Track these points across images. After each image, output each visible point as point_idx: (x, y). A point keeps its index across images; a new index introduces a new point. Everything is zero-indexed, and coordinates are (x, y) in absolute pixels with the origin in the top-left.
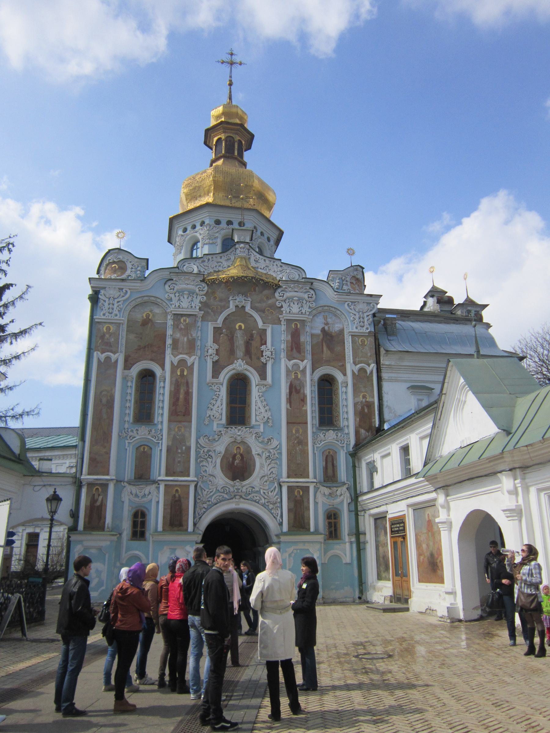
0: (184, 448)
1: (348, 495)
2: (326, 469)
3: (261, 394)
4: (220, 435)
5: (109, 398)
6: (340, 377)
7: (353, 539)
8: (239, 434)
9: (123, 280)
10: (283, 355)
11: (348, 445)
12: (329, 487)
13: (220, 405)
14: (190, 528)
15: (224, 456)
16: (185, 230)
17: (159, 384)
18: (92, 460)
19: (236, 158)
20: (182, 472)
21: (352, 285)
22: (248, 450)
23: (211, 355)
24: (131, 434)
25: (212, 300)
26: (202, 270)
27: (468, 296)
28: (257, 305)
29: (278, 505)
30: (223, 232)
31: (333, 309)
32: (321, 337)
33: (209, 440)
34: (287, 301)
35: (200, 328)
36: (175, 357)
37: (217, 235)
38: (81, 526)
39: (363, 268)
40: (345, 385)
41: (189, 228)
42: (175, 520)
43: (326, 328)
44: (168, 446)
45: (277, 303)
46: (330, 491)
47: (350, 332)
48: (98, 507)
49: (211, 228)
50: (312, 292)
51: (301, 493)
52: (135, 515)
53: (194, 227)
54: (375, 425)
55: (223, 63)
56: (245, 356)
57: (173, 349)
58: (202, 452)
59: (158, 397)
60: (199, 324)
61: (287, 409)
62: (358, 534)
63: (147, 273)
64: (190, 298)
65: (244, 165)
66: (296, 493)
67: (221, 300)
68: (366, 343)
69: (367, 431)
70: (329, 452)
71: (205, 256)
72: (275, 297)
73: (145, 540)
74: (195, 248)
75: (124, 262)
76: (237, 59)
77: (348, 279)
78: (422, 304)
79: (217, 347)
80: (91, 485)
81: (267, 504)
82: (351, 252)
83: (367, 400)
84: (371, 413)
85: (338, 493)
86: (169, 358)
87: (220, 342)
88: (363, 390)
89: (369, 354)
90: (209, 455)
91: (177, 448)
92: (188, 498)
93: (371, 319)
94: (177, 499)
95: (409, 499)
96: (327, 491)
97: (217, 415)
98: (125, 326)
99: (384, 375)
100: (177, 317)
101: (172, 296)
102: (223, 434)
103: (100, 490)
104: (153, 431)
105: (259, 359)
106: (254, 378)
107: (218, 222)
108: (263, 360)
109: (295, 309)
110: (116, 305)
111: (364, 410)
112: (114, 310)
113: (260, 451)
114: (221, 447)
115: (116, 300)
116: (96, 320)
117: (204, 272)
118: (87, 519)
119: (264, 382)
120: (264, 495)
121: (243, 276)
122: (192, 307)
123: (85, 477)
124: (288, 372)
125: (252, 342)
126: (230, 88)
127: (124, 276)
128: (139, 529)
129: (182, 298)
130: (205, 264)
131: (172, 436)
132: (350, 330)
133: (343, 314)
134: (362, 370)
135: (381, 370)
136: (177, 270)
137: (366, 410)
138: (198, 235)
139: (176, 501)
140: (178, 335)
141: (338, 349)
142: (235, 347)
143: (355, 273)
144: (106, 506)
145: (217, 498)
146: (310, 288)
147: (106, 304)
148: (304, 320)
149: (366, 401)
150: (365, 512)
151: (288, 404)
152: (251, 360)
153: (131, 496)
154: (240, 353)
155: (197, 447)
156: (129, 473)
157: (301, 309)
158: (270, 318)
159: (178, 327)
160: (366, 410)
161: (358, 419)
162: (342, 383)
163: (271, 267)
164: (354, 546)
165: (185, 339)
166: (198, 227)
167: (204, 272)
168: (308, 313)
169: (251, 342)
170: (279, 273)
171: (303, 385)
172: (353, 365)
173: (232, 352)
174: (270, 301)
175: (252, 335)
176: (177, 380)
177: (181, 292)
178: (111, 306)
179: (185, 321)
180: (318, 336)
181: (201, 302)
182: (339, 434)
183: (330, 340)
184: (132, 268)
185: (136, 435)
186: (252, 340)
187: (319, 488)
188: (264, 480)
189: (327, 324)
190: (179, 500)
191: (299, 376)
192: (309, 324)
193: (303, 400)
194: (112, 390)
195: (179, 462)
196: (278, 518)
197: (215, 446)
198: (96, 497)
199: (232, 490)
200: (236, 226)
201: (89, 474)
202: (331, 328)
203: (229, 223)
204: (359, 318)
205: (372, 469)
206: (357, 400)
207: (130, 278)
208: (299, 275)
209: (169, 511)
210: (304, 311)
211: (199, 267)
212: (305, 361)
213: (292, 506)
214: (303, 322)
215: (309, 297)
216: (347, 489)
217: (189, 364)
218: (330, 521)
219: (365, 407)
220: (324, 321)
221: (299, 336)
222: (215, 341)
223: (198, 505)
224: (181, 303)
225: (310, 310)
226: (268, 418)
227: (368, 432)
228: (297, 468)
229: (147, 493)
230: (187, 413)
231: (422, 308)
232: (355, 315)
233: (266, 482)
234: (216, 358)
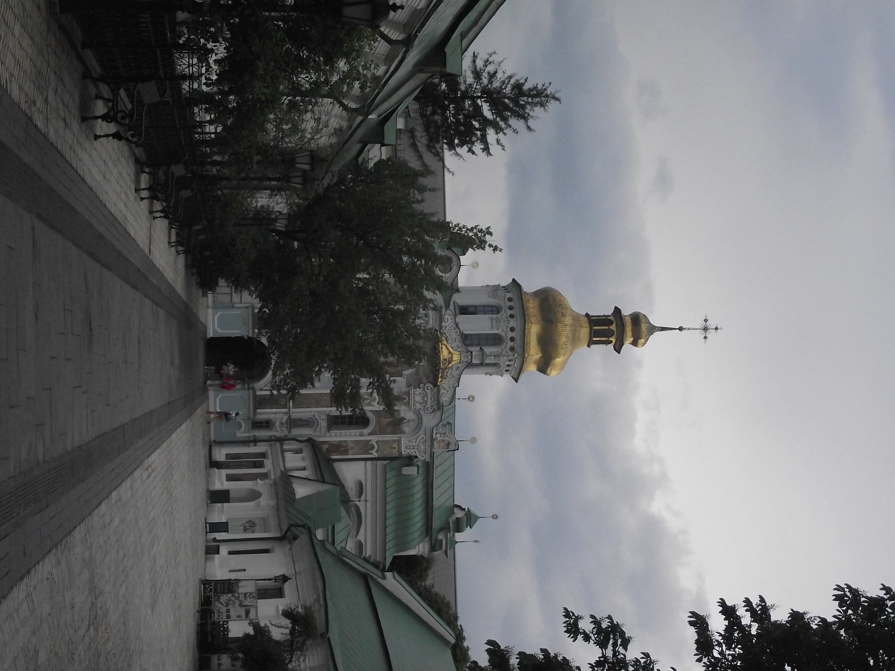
6: (366, 431)
7: (252, 439)
11: (317, 436)
16: (510, 300)
30: (503, 334)
53: (511, 308)
55: (706, 321)
62: (256, 441)
65: (588, 346)
69: (327, 450)
76: (711, 334)
77: (446, 438)
96: (284, 421)
99: (369, 463)
107: (512, 329)
134: (373, 447)
166: (510, 312)
174: (424, 379)
180: (399, 414)
200: (510, 344)
203: (512, 339)
214: (408, 404)
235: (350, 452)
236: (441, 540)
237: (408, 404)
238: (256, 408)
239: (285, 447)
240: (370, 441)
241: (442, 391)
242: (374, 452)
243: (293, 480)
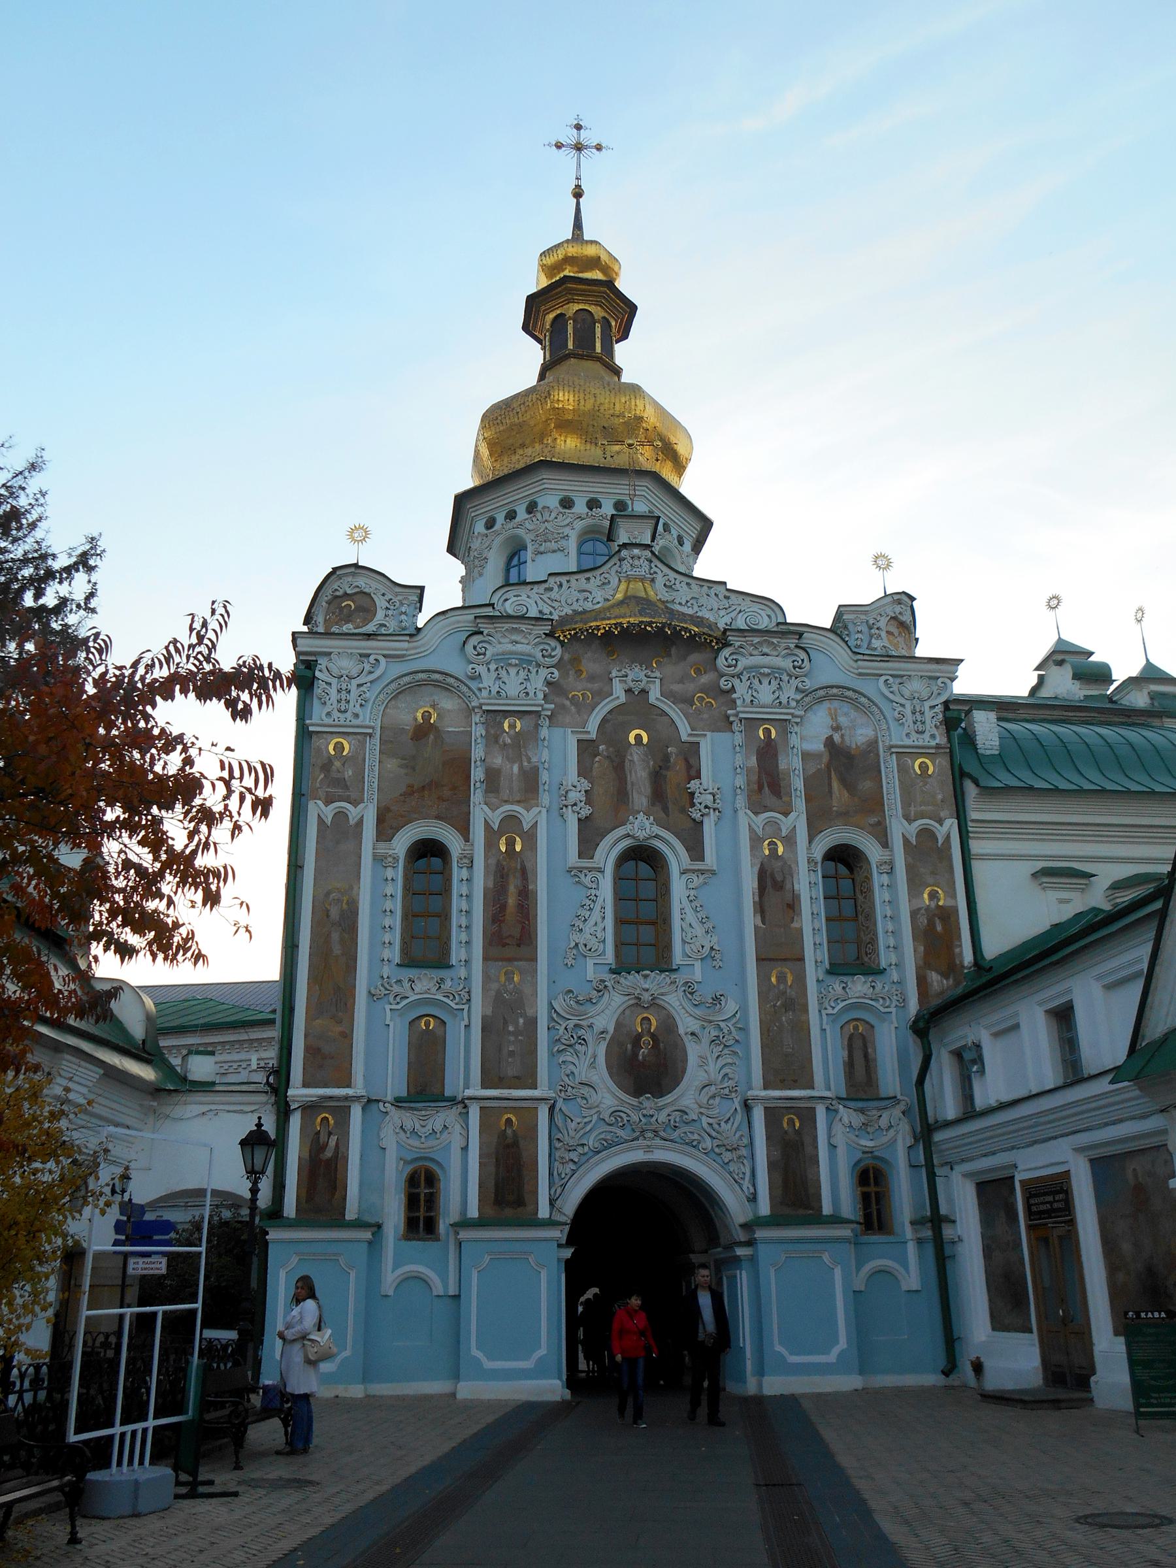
0: (521, 1021)
1: (907, 1128)
2: (850, 1065)
3: (692, 893)
4: (601, 988)
5: (345, 906)
6: (873, 851)
7: (928, 1233)
8: (647, 986)
9: (369, 636)
10: (741, 801)
12: (862, 1111)
13: (599, 920)
14: (544, 1212)
15: (612, 1038)
16: (490, 523)
17: (458, 873)
18: (312, 1051)
19: (598, 359)
20: (517, 1078)
21: (891, 638)
22: (669, 1025)
23: (575, 804)
24: (396, 989)
25: (571, 678)
26: (546, 610)
27: (1147, 660)
28: (676, 687)
29: (744, 1152)
30: (579, 525)
31: (850, 693)
32: (825, 759)
33: (577, 1002)
34: (744, 678)
35: (546, 743)
36: (493, 810)
37: (567, 531)
38: (290, 1207)
39: (913, 599)
40: (886, 868)
41: (500, 518)
42: (508, 1191)
43: (837, 738)
44: (483, 1018)
45: (722, 682)
46: (862, 1119)
47: (892, 747)
48: (329, 1161)
49: (553, 515)
50: (803, 655)
51: (797, 1125)
52: (412, 1180)
53: (511, 515)
54: (962, 962)
55: (559, 146)
56: (653, 804)
57: (486, 791)
58: (562, 1029)
59: (457, 904)
60: (544, 732)
61: (756, 927)
62: (935, 1220)
63: (421, 621)
64: (523, 674)
65: (617, 372)
66: (785, 1125)
67: (592, 678)
68: (930, 772)
69: (945, 975)
70: (856, 1028)
71: (552, 580)
72: (715, 668)
73: (438, 1240)
74: (515, 562)
75: (369, 594)
77: (882, 623)
78: (1034, 681)
79: (585, 785)
80: (310, 1109)
81: (717, 1150)
82: (882, 562)
83: (941, 903)
84: (952, 933)
85: (883, 1122)
86: (481, 814)
87: (594, 774)
88: (931, 880)
89: (940, 797)
90: (579, 1038)
91: (506, 1023)
92: (535, 1139)
93: (941, 716)
94: (509, 1141)
95: (1078, 1135)
97: (593, 943)
98: (377, 740)
99: (975, 846)
100: (494, 717)
101: (482, 669)
102: (611, 988)
103: (332, 1122)
104: (449, 983)
105: (683, 811)
106: (676, 856)
107: (567, 503)
108: (696, 815)
109: (766, 694)
110: (355, 692)
111: (934, 927)
112: (352, 704)
113: (694, 1025)
114: (605, 1016)
115: (355, 682)
116: (311, 729)
117: (551, 613)
118: (304, 1194)
119: (698, 865)
120: (709, 1130)
121: (641, 622)
122: (527, 694)
123: (297, 1092)
124: (756, 841)
125: (669, 773)
126: (578, 204)
127: (370, 628)
128: (422, 1216)
129: (503, 673)
130: (553, 595)
131: (493, 993)
132: (894, 742)
133: (876, 705)
134: (926, 834)
135: (968, 832)
136: (488, 611)
137: (939, 928)
138: (521, 532)
139: (508, 1146)
140: (498, 761)
141: (866, 785)
142: (629, 787)
143: (898, 609)
144: (346, 1159)
145: (589, 1139)
146: (797, 647)
147: (333, 691)
148: (786, 720)
149: (938, 907)
150: (952, 1169)
151: (759, 918)
152: (668, 815)
153: (402, 1133)
154: (640, 797)
155: (551, 1019)
156: (394, 1080)
157: (777, 694)
158: (705, 716)
159: (497, 742)
160: (939, 928)
161: (922, 948)
162: (880, 864)
163: (702, 601)
164: (930, 1250)
165: (516, 768)
166: (522, 514)
167: (551, 613)
168: (793, 704)
169: (664, 772)
170: (722, 613)
171: (788, 871)
172: (905, 823)
173: (622, 795)
174: (705, 679)
175: (666, 758)
176: (498, 864)
177: (503, 662)
178: (344, 695)
179: (512, 726)
181: (549, 684)
182: (879, 986)
183: (846, 765)
184: (387, 608)
185: (409, 993)
186: (668, 768)
187: (836, 1111)
188: (710, 1094)
189: (837, 728)
190: (515, 1144)
191: (780, 850)
192: (796, 729)
193: (792, 906)
194: (351, 888)
195: (511, 1054)
196: (746, 1184)
197: (591, 1017)
198: (323, 1138)
199: (635, 1118)
201: (305, 1085)
202: (847, 738)
203: (593, 504)
204: (914, 713)
205: (969, 1062)
206: (917, 904)
207: (383, 630)
208: (769, 616)
209: (492, 1169)
210: (784, 701)
211: (540, 603)
212: (793, 815)
213: (777, 1154)
214: (783, 725)
215: (794, 667)
216: (903, 1113)
217: (526, 827)
218: (866, 1189)
219: (937, 921)
220: (829, 722)
221: (775, 756)
222: (583, 772)
223: (558, 1154)
224: (502, 685)
225: (798, 697)
226: (712, 948)
227: (947, 978)
228: (786, 1064)
229: (438, 1128)
230: (526, 938)
231: (1034, 691)
232: (903, 706)
233: (713, 1097)
234: (586, 811)
235: (950, 903)
236: (1153, 696)
237: (783, 725)
238: (816, 1218)
239: (951, 1110)
240: (906, 841)
241: (740, 624)
242: (941, 831)
243: (1156, 1029)
